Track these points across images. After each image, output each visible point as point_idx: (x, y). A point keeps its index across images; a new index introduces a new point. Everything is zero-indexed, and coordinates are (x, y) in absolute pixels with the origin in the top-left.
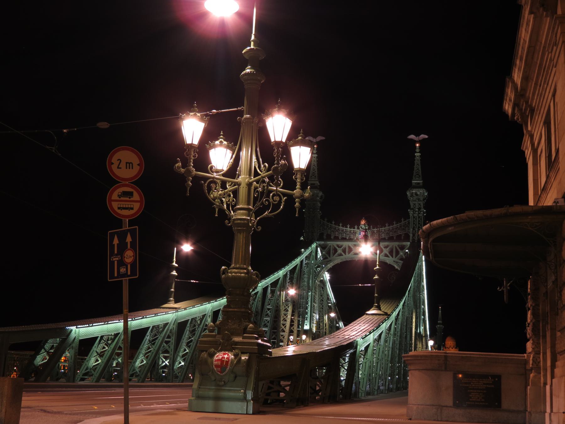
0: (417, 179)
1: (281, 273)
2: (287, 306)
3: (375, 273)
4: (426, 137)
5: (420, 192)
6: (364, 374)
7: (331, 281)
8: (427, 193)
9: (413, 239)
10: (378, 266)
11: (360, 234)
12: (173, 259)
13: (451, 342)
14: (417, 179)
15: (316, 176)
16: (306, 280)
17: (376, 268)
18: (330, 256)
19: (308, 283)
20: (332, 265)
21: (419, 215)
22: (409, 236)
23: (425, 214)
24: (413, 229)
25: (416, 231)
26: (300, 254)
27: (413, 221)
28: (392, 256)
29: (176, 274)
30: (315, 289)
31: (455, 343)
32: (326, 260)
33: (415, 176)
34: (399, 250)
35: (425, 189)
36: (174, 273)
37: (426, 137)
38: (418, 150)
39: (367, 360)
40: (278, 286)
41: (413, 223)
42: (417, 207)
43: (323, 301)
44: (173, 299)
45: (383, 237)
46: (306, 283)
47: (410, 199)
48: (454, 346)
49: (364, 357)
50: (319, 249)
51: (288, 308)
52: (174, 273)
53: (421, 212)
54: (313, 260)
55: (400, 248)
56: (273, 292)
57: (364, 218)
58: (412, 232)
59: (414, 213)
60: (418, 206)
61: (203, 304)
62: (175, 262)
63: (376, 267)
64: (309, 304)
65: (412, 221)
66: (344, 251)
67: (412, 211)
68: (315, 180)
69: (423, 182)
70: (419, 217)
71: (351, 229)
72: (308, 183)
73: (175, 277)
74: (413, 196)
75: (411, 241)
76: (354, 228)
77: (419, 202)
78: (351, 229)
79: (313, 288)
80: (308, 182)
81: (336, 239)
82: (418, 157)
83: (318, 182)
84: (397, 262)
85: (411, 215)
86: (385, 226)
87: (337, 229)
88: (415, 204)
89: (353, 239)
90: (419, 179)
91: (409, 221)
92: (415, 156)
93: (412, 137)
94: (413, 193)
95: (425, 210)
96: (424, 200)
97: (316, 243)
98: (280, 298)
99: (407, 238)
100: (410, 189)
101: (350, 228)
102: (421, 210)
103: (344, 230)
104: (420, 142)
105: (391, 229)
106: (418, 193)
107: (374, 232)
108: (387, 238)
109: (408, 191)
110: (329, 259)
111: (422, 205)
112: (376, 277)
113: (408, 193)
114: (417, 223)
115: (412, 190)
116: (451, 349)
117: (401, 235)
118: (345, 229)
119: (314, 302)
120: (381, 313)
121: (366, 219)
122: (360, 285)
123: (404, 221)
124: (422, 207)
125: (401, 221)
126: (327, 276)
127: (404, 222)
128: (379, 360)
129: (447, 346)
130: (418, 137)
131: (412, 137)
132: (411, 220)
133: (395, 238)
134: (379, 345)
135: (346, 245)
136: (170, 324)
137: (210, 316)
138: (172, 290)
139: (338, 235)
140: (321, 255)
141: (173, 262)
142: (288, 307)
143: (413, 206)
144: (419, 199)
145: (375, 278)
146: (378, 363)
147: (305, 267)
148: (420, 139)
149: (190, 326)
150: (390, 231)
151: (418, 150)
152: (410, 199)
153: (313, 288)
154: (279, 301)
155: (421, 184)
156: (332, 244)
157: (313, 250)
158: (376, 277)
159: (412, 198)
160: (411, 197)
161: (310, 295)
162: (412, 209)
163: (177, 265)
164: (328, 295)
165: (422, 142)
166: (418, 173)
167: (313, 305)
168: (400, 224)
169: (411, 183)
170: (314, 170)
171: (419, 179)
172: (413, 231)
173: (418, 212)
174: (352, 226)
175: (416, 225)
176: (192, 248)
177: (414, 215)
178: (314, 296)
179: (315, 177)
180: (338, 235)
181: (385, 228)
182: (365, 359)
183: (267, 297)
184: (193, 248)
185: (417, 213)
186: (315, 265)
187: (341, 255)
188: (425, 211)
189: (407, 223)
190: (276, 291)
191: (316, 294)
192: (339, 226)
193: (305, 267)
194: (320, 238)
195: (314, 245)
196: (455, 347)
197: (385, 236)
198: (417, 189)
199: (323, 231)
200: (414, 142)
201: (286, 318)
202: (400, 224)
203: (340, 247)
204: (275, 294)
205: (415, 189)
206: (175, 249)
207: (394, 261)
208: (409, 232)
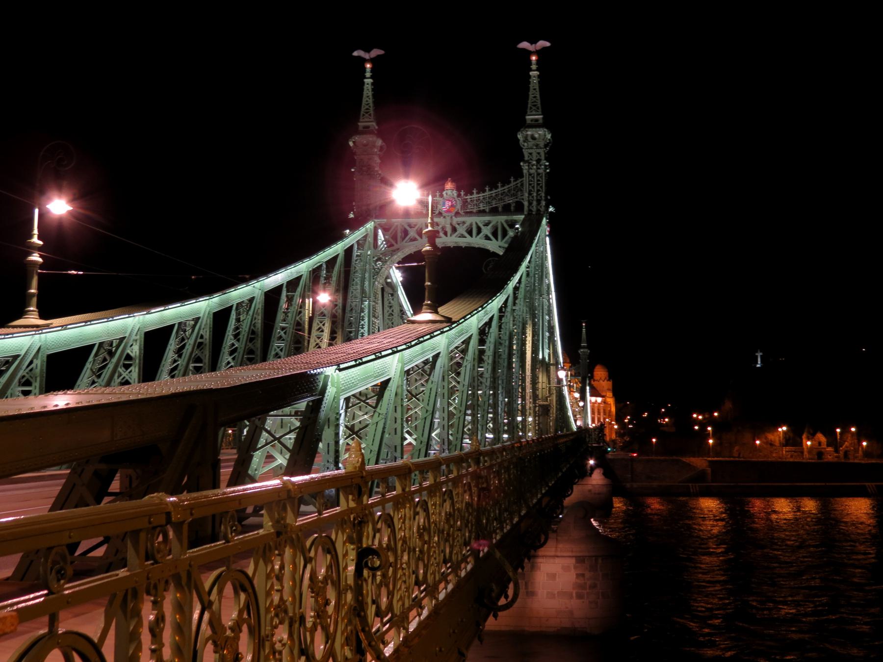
0: (534, 113)
1: (303, 267)
2: (321, 322)
4: (548, 44)
5: (539, 134)
6: (371, 451)
7: (404, 284)
9: (530, 210)
11: (444, 205)
12: (32, 229)
13: (602, 373)
16: (358, 280)
17: (427, 230)
18: (396, 242)
19: (361, 286)
20: (402, 257)
21: (539, 170)
22: (523, 205)
23: (547, 169)
24: (530, 194)
25: (533, 197)
26: (341, 237)
27: (529, 181)
28: (497, 239)
29: (40, 260)
30: (375, 297)
31: (607, 373)
32: (391, 249)
33: (531, 108)
34: (507, 228)
35: (547, 129)
36: (36, 257)
37: (548, 44)
38: (534, 67)
39: (380, 418)
40: (299, 289)
42: (535, 158)
43: (393, 315)
44: (35, 309)
45: (482, 208)
46: (359, 287)
47: (524, 146)
48: (606, 378)
49: (375, 412)
50: (380, 232)
51: (323, 327)
52: (36, 257)
53: (541, 165)
54: (369, 249)
56: (290, 300)
58: (527, 199)
59: (530, 168)
60: (537, 156)
61: (115, 318)
64: (366, 320)
65: (527, 180)
67: (527, 164)
68: (371, 120)
69: (543, 118)
70: (538, 174)
72: (358, 126)
73: (38, 266)
74: (527, 140)
75: (526, 213)
77: (538, 151)
79: (372, 295)
80: (359, 124)
82: (534, 77)
83: (374, 124)
85: (525, 171)
88: (531, 154)
90: (537, 113)
91: (522, 181)
92: (530, 77)
93: (524, 45)
94: (527, 135)
95: (548, 162)
96: (546, 146)
97: (374, 222)
98: (305, 309)
99: (519, 209)
100: (522, 129)
102: (541, 163)
104: (537, 52)
105: (494, 195)
106: (536, 136)
107: (467, 201)
108: (487, 210)
109: (520, 133)
110: (396, 246)
113: (520, 136)
114: (536, 184)
116: (601, 381)
117: (509, 205)
119: (374, 316)
120: (438, 318)
121: (453, 181)
123: (515, 181)
124: (543, 157)
125: (509, 182)
126: (397, 276)
127: (515, 183)
128: (428, 413)
129: (595, 378)
130: (534, 45)
131: (524, 45)
132: (526, 180)
133: (500, 209)
134: (430, 382)
136: (22, 358)
137: (138, 341)
140: (383, 239)
141: (31, 236)
142: (324, 325)
143: (529, 157)
144: (537, 146)
145: (424, 249)
146: (425, 418)
147: (356, 261)
148: (538, 48)
149: (94, 360)
150: (493, 200)
151: (534, 67)
152: (522, 146)
153: (372, 295)
154: (302, 314)
155: (541, 121)
157: (369, 233)
159: (526, 144)
160: (524, 141)
161: (367, 306)
162: (527, 162)
163: (41, 243)
164: (401, 306)
165: (540, 53)
166: (535, 104)
167: (373, 321)
168: (507, 187)
169: (525, 120)
170: (367, 104)
171: (537, 113)
172: (529, 197)
173: (537, 166)
176: (70, 208)
177: (531, 171)
178: (374, 307)
179: (370, 115)
182: (376, 414)
183: (279, 309)
184: (71, 208)
185: (535, 167)
186: (374, 258)
187: (415, 239)
188: (547, 164)
189: (519, 185)
190: (295, 298)
191: (377, 303)
193: (356, 261)
195: (370, 225)
196: (608, 379)
198: (534, 129)
200: (529, 53)
201: (320, 343)
202: (507, 187)
204: (293, 303)
205: (530, 129)
207: (500, 247)
208: (523, 199)
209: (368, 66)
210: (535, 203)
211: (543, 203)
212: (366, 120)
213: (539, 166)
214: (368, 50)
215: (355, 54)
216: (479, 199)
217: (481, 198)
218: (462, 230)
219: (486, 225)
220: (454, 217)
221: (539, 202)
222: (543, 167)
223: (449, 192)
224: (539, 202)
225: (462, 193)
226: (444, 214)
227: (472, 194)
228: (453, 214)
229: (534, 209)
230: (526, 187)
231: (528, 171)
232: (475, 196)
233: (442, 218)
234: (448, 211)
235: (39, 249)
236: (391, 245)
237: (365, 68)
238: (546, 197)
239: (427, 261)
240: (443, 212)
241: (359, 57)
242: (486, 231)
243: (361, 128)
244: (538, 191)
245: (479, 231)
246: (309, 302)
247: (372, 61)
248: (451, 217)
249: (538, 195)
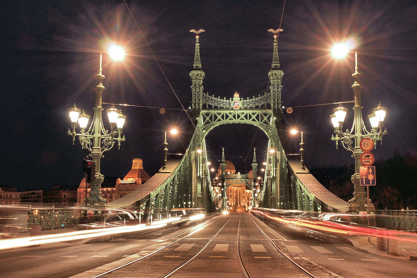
3: (300, 147)
4: (282, 30)
8: (283, 74)
9: (274, 108)
10: (303, 142)
11: (234, 104)
12: (165, 140)
14: (276, 63)
15: (199, 60)
21: (278, 90)
24: (274, 100)
25: (275, 102)
27: (274, 94)
37: (282, 30)
41: (274, 96)
42: (276, 84)
45: (251, 106)
52: (166, 149)
55: (264, 114)
57: (236, 92)
58: (273, 103)
62: (166, 142)
63: (301, 143)
66: (223, 117)
70: (278, 91)
71: (227, 101)
74: (273, 75)
76: (229, 100)
77: (278, 80)
78: (227, 101)
80: (194, 65)
81: (216, 108)
83: (201, 65)
84: (262, 125)
85: (272, 90)
86: (252, 98)
87: (216, 100)
89: (229, 108)
92: (274, 45)
94: (273, 73)
103: (222, 101)
104: (277, 34)
106: (277, 73)
108: (254, 107)
109: (270, 72)
110: (212, 123)
111: (280, 82)
112: (301, 149)
115: (273, 71)
121: (238, 92)
122: (291, 154)
124: (280, 84)
131: (271, 30)
138: (165, 160)
139: (217, 105)
144: (277, 78)
155: (279, 67)
156: (213, 112)
158: (301, 149)
171: (277, 63)
175: (276, 97)
180: (217, 105)
181: (252, 100)
185: (276, 88)
186: (201, 128)
187: (219, 120)
192: (218, 98)
194: (204, 107)
197: (252, 106)
199: (206, 102)
200: (273, 34)
203: (220, 114)
206: (166, 133)
209: (197, 37)
210: (276, 105)
211: (280, 105)
212: (197, 63)
213: (278, 88)
214: (197, 30)
215: (191, 31)
216: (250, 102)
217: (251, 101)
218: (242, 116)
219: (253, 114)
221: (278, 104)
222: (280, 88)
223: (236, 98)
224: (278, 104)
225: (242, 99)
226: (234, 109)
227: (246, 99)
229: (276, 108)
230: (272, 97)
231: (273, 90)
232: (248, 100)
234: (236, 107)
235: (167, 146)
236: (208, 123)
237: (196, 38)
238: (281, 102)
239: (301, 153)
241: (192, 33)
242: (254, 117)
243: (194, 67)
244: (278, 99)
245: (250, 117)
246: (193, 153)
247: (200, 35)
249: (278, 101)
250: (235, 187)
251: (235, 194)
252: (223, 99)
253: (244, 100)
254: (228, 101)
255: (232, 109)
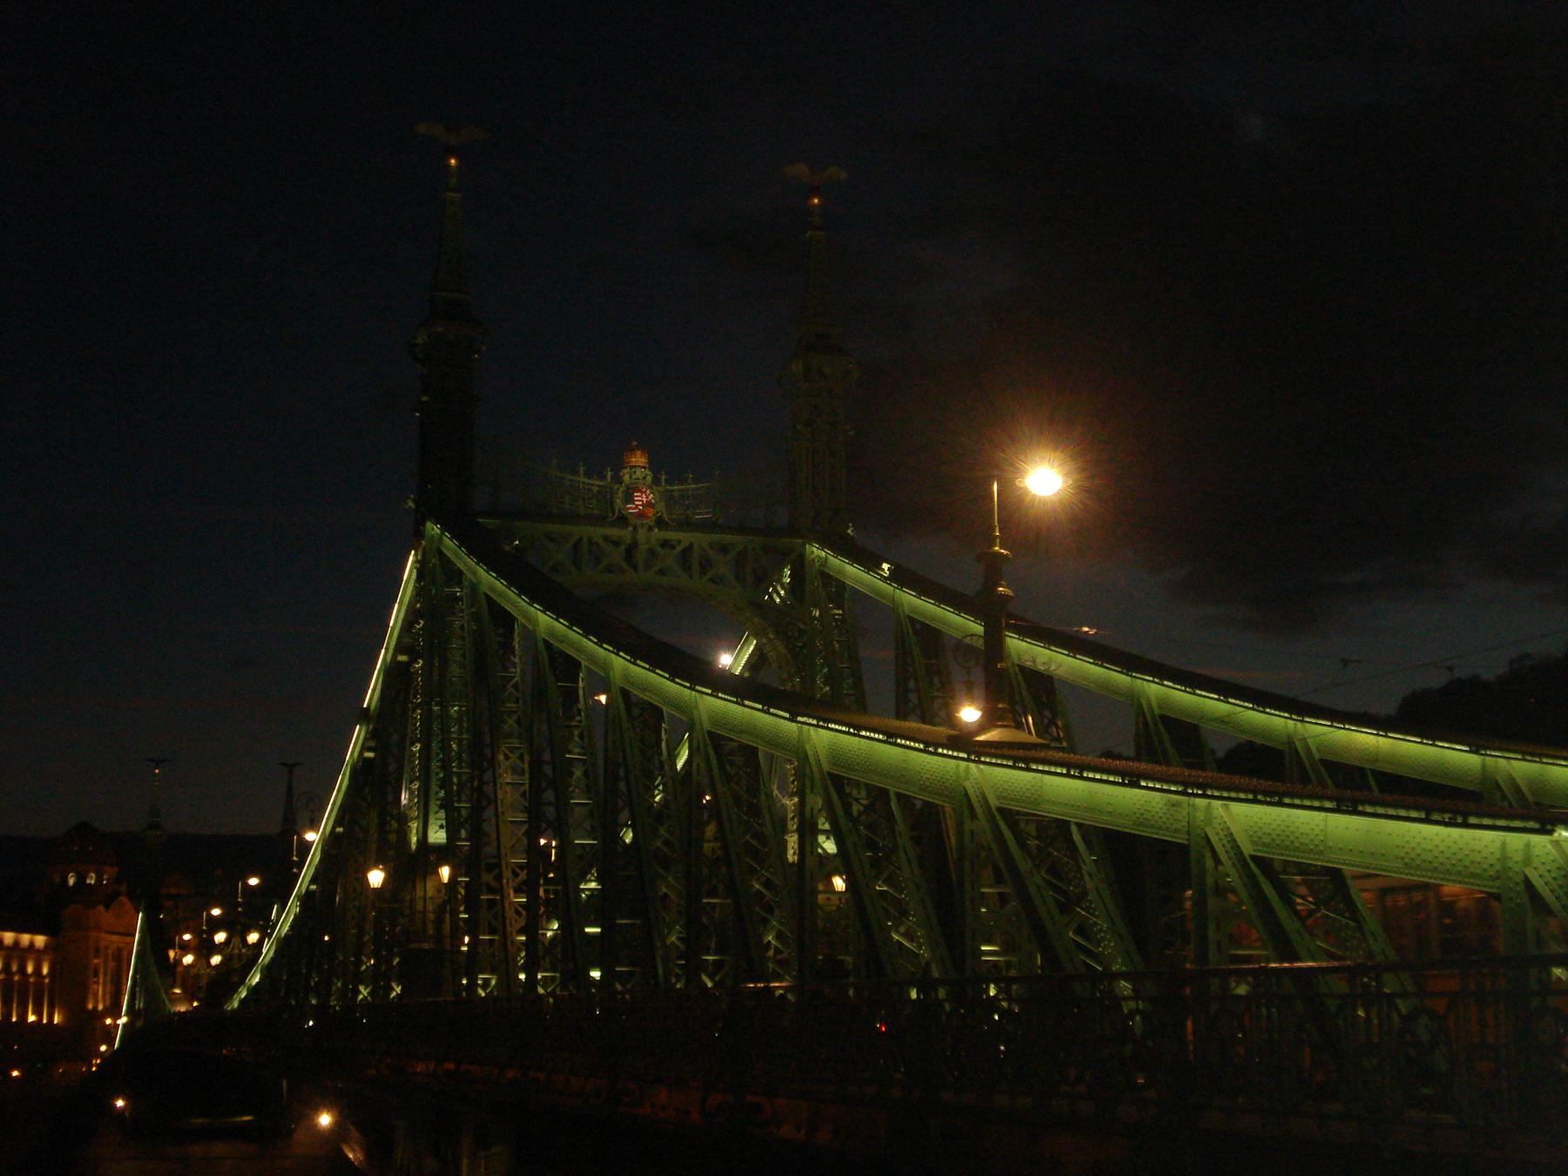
4: (844, 175)
11: (629, 498)
76: (603, 477)
93: (800, 170)
101: (588, 474)
106: (827, 370)
118: (570, 480)
131: (800, 170)
135: (581, 538)
174: (595, 471)
215: (422, 129)
219: (724, 549)
220: (656, 530)
226: (630, 522)
228: (652, 524)
233: (630, 529)
234: (641, 515)
240: (630, 516)
245: (705, 565)
248: (650, 529)
250: (114, 938)
251: (112, 964)
252: (575, 472)
253: (669, 482)
254: (596, 483)
255: (623, 520)
